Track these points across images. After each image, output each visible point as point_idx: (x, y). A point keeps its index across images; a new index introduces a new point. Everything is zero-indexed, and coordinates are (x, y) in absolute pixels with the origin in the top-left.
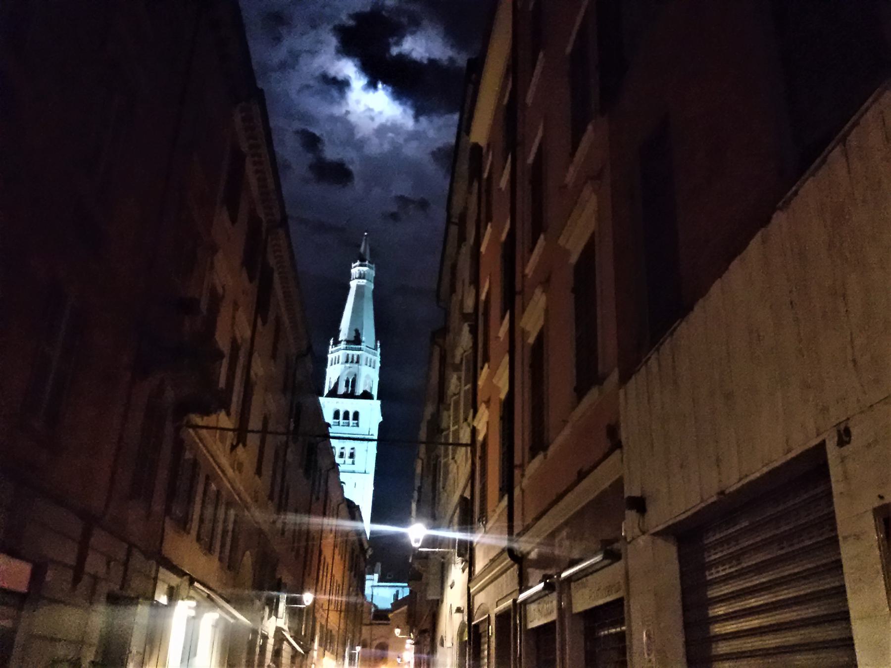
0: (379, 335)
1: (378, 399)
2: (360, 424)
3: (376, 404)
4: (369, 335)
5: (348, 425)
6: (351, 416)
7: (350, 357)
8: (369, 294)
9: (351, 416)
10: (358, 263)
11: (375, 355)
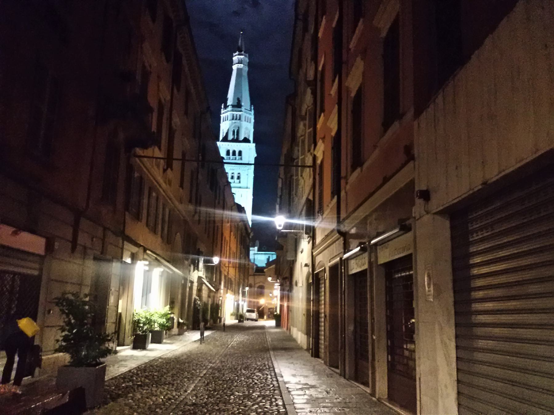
0: (252, 103)
1: (254, 142)
2: (243, 159)
3: (252, 146)
4: (246, 101)
5: (236, 159)
7: (235, 115)
8: (245, 74)
10: (237, 53)
11: (250, 114)
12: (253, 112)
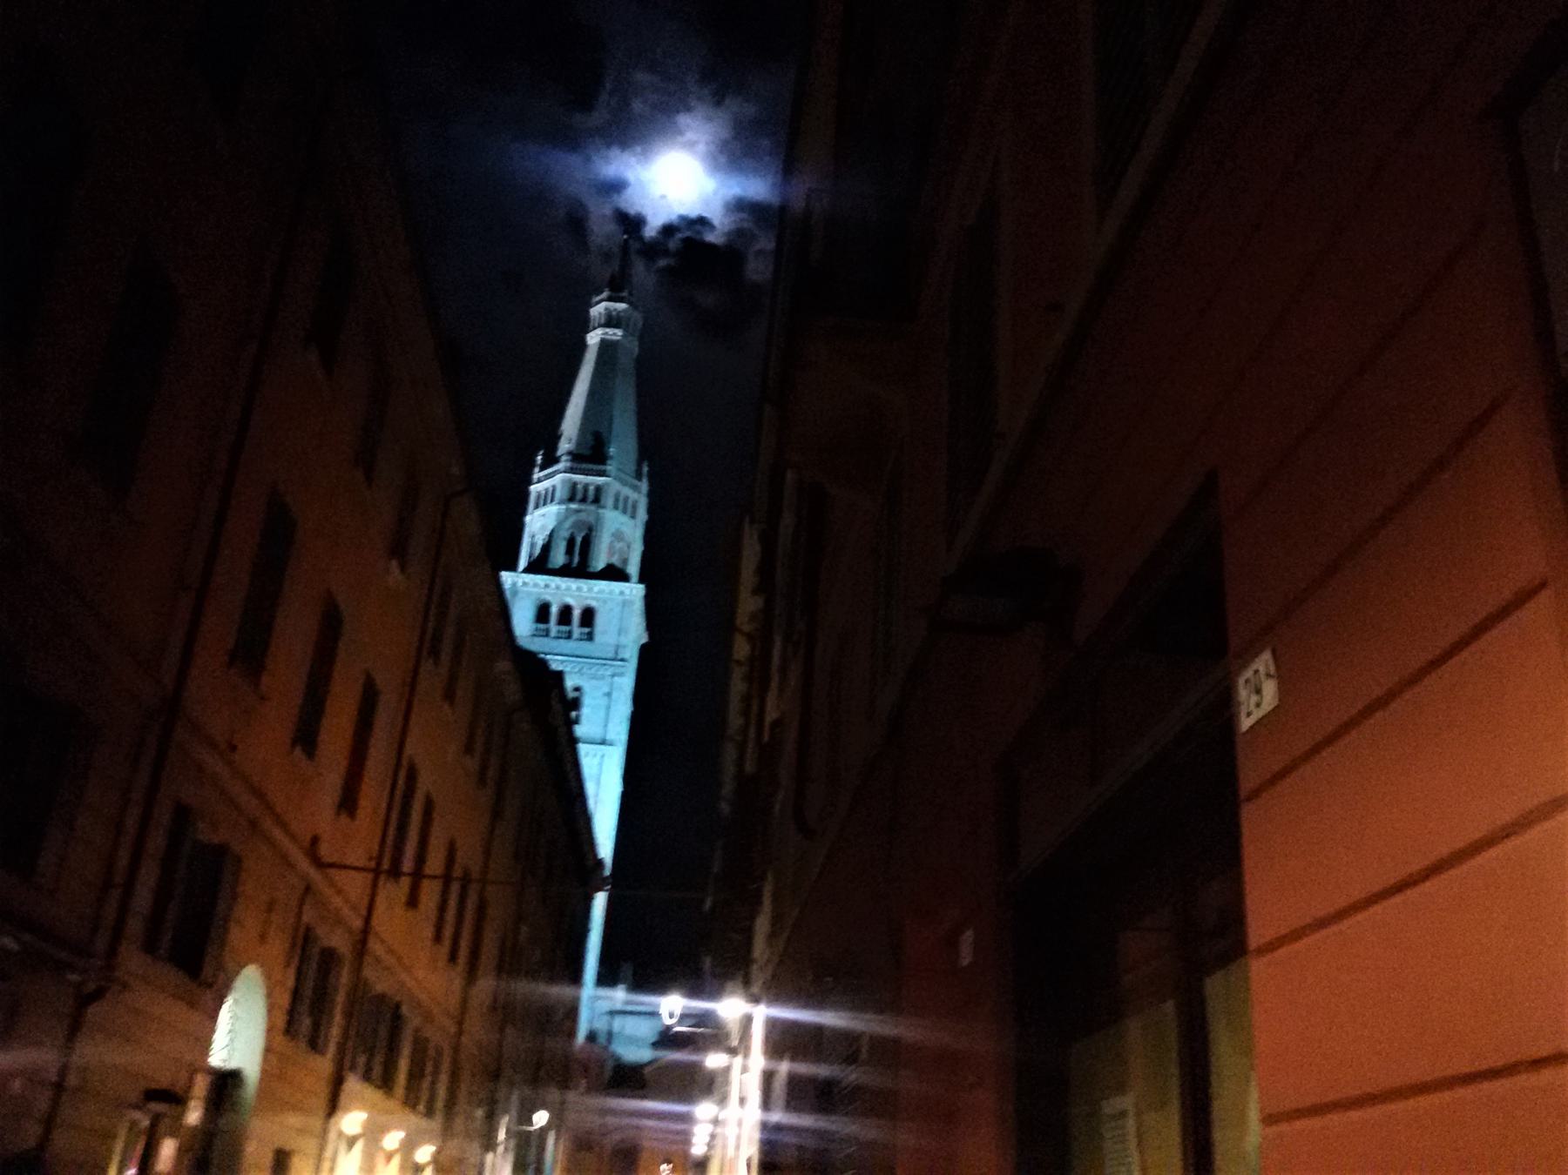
0: (647, 451)
1: (641, 581)
2: (598, 637)
3: (634, 591)
4: (623, 447)
6: (576, 613)
8: (626, 362)
9: (576, 613)
10: (605, 295)
11: (635, 488)
12: (644, 486)
